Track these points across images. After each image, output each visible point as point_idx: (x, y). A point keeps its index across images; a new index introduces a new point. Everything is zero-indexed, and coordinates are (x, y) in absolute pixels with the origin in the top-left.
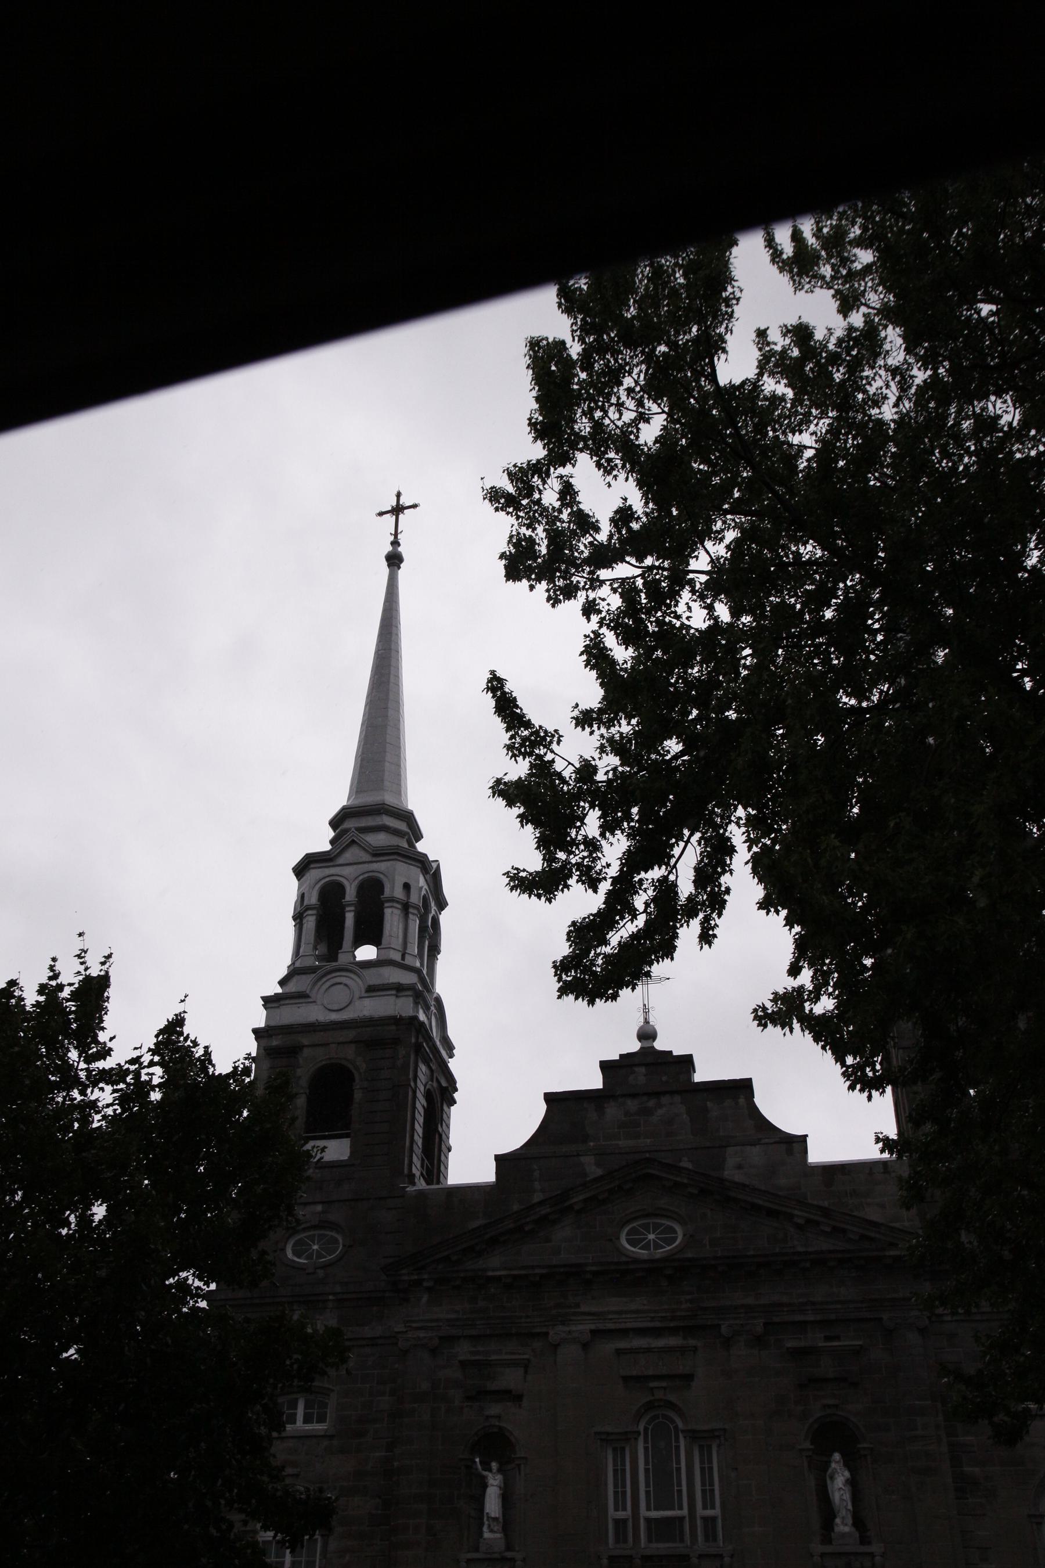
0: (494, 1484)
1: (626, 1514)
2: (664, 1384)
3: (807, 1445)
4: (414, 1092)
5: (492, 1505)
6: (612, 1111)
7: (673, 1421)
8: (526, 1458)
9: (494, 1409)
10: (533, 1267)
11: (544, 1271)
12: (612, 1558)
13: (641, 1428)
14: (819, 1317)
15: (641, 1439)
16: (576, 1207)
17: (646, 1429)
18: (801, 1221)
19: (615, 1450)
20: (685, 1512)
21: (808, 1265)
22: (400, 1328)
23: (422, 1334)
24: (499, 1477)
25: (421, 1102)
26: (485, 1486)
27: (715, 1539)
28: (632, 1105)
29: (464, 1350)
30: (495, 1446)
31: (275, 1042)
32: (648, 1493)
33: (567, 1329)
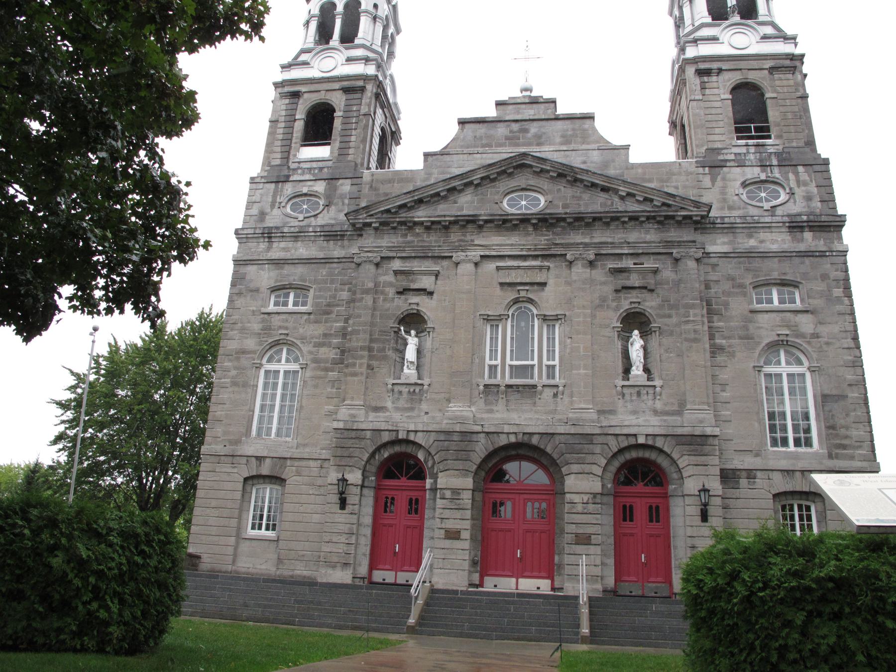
0: (412, 343)
2: (527, 288)
3: (619, 325)
4: (373, 121)
5: (411, 354)
6: (501, 131)
7: (531, 311)
9: (414, 299)
10: (445, 216)
14: (631, 251)
15: (509, 320)
16: (475, 182)
18: (624, 194)
19: (492, 326)
20: (535, 362)
21: (626, 219)
22: (356, 251)
23: (370, 255)
24: (416, 340)
25: (377, 131)
26: (406, 344)
27: (554, 378)
28: (515, 127)
30: (413, 321)
31: (286, 89)
32: (512, 351)
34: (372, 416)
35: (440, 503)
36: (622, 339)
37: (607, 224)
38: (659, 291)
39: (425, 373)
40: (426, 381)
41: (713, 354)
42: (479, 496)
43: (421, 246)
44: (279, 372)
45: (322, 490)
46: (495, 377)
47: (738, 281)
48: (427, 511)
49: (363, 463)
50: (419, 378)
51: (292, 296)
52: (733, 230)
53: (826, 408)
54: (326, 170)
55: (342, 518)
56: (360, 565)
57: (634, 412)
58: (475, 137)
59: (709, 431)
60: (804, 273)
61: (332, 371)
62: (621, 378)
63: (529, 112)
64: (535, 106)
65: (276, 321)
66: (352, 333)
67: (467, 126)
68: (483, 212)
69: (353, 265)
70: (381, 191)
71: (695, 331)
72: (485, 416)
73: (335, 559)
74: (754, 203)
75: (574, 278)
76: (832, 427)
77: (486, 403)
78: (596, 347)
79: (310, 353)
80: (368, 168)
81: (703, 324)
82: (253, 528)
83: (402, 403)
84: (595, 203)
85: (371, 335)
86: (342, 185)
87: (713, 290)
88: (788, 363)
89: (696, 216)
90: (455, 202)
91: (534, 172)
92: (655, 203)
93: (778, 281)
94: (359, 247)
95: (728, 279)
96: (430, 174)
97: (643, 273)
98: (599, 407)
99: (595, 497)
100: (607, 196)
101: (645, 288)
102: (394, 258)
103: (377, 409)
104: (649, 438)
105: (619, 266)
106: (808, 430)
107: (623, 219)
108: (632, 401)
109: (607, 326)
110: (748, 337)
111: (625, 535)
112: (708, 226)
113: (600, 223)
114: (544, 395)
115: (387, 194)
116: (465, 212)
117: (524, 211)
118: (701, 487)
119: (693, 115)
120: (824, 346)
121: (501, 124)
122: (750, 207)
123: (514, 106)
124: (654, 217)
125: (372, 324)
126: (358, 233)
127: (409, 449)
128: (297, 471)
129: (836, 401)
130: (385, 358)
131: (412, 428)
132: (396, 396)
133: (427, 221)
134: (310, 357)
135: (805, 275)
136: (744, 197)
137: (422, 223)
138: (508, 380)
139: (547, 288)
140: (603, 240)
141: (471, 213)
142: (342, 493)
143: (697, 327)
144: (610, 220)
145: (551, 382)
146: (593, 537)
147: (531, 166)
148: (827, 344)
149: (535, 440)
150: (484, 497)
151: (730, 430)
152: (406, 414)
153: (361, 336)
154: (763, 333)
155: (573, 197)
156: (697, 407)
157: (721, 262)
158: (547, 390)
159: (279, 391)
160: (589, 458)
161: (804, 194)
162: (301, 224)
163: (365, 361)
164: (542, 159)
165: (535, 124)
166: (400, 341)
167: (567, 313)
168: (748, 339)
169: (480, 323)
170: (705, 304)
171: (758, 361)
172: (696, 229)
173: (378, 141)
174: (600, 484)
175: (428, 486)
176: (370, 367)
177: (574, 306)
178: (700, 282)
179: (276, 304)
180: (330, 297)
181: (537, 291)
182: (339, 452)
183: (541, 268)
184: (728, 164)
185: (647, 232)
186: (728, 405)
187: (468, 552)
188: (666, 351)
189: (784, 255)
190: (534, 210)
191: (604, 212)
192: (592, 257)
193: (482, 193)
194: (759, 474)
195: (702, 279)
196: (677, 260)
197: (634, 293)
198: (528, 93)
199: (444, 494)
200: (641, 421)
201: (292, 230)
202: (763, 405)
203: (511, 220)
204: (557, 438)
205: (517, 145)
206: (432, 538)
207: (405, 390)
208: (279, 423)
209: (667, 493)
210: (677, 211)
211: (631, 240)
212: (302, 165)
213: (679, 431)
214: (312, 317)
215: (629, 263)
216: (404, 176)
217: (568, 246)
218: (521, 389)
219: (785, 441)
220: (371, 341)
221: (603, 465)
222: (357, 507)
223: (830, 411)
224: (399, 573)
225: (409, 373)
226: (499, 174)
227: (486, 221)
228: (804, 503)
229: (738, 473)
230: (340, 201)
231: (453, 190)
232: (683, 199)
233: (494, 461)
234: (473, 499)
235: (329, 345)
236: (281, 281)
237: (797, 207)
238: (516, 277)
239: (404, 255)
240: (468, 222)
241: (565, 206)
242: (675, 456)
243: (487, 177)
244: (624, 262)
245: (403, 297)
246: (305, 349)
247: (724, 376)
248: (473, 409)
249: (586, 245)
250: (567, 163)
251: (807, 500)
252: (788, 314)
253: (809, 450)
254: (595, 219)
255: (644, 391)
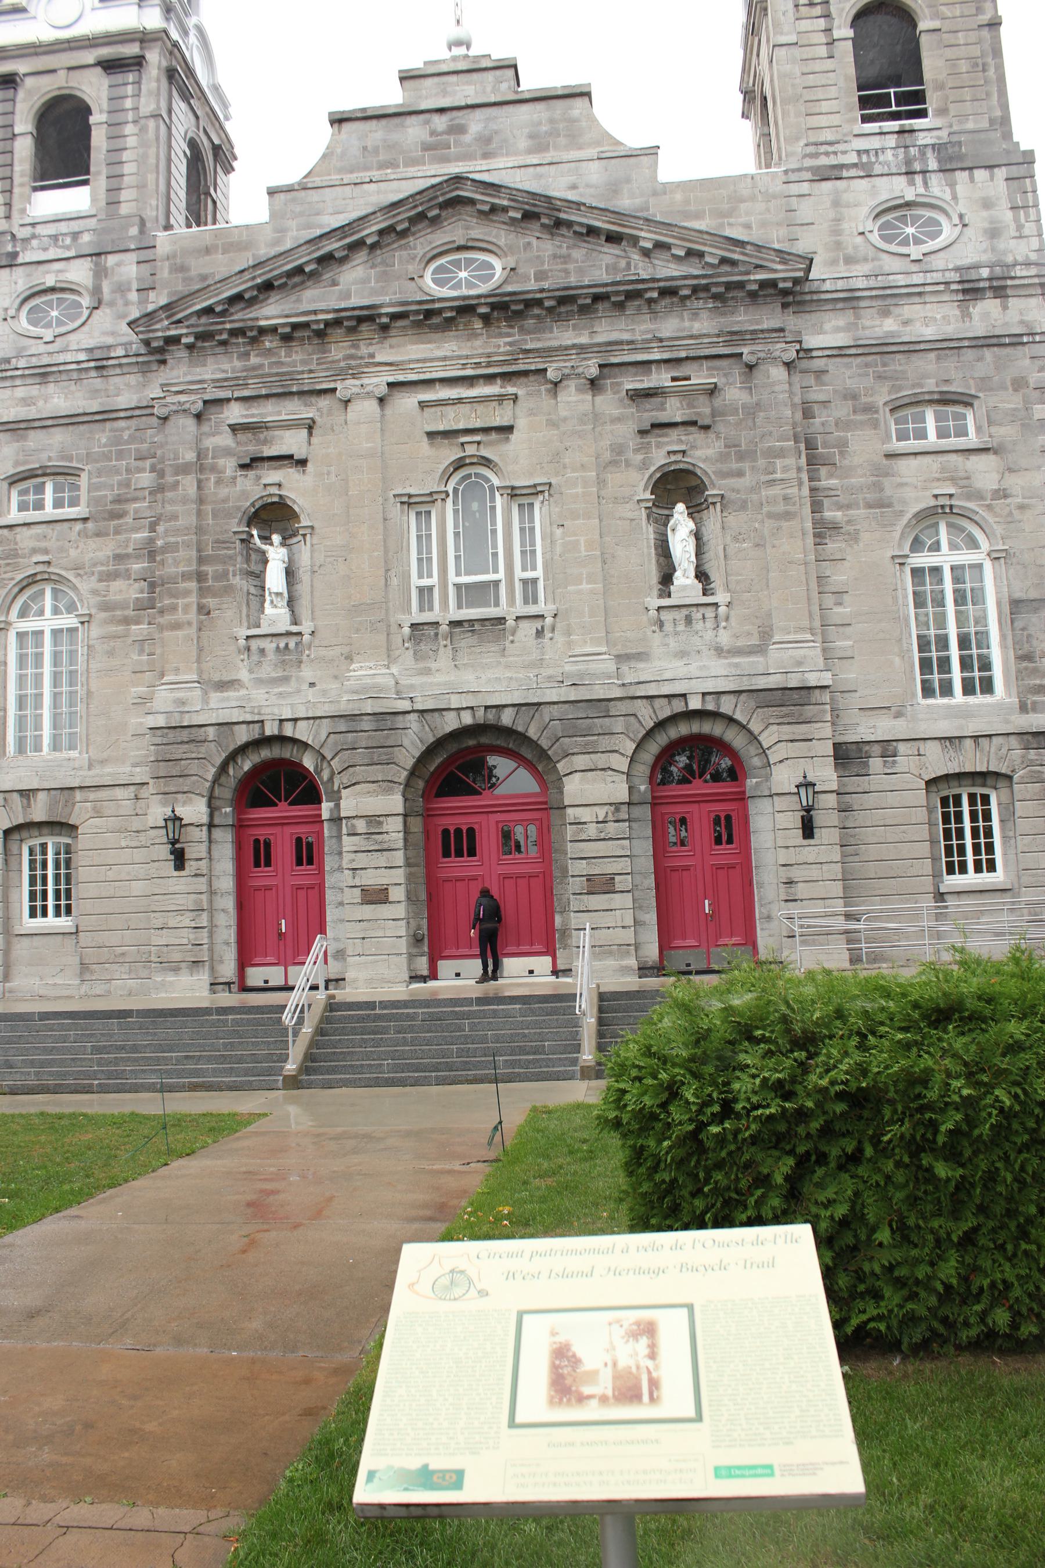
1: (434, 581)
2: (477, 438)
3: (648, 495)
4: (169, 128)
5: (275, 579)
6: (414, 132)
7: (488, 480)
8: (312, 527)
9: (272, 476)
10: (315, 312)
11: (330, 316)
12: (414, 626)
13: (450, 488)
14: (666, 356)
15: (450, 501)
16: (369, 241)
17: (456, 490)
18: (649, 245)
19: (418, 514)
20: (501, 575)
21: (655, 295)
22: (157, 393)
23: (182, 398)
24: (283, 551)
25: (180, 147)
26: (266, 562)
27: (535, 601)
28: (440, 122)
29: (235, 413)
30: (274, 516)
32: (457, 558)
33: (357, 382)
34: (215, 697)
35: (349, 843)
36: (656, 521)
37: (620, 306)
38: (720, 427)
39: (304, 613)
40: (306, 627)
41: (819, 537)
42: (417, 825)
43: (277, 374)
44: (42, 632)
45: (142, 837)
46: (431, 609)
47: (864, 400)
48: (327, 858)
49: (208, 785)
50: (295, 623)
51: (49, 488)
52: (855, 304)
53: (1019, 624)
54: (86, 238)
55: (180, 883)
56: (222, 962)
57: (682, 654)
58: (365, 148)
59: (813, 680)
60: (982, 379)
61: (138, 623)
62: (655, 592)
63: (466, 90)
64: (475, 76)
65: (25, 539)
66: (167, 548)
67: (347, 127)
68: (388, 298)
69: (154, 421)
70: (193, 273)
71: (786, 498)
72: (416, 680)
73: (176, 956)
74: (893, 248)
75: (563, 413)
76: (1028, 657)
77: (418, 656)
78: (607, 539)
79: (95, 592)
80: (168, 227)
81: (800, 484)
82: (33, 914)
83: (268, 670)
84: (598, 267)
85: (199, 551)
86: (119, 264)
87: (817, 420)
88: (953, 546)
89: (784, 280)
90: (335, 283)
91: (480, 212)
92: (708, 259)
93: (936, 397)
94: (162, 385)
95: (845, 398)
96: (282, 231)
97: (688, 395)
98: (619, 650)
99: (617, 810)
100: (617, 252)
101: (694, 423)
102: (228, 400)
103: (223, 685)
104: (708, 698)
105: (645, 385)
106: (986, 665)
107: (648, 295)
108: (676, 633)
109: (626, 500)
110: (881, 504)
111: (674, 869)
112: (808, 297)
113: (607, 305)
114: (520, 634)
115: (204, 278)
116: (355, 301)
117: (465, 292)
118: (801, 779)
119: (779, 77)
120: (1015, 512)
121: (414, 118)
122: (884, 256)
123: (436, 80)
124: (706, 288)
125: (200, 530)
126: (158, 357)
127: (287, 753)
128: (94, 809)
129: (1036, 610)
130: (229, 590)
131: (287, 714)
132: (255, 658)
133: (284, 325)
134: (94, 600)
135: (984, 383)
136: (875, 238)
137: (274, 329)
138: (456, 614)
139: (513, 437)
140: (615, 336)
141: (366, 302)
142: (174, 842)
143: (789, 491)
144: (625, 298)
145: (532, 610)
146: (617, 878)
147: (472, 202)
148: (1022, 507)
149: (507, 718)
150: (426, 825)
151: (850, 674)
152: (276, 690)
153: (182, 553)
154: (909, 493)
155: (555, 256)
156: (791, 637)
157: (832, 365)
158: (524, 624)
159: (47, 669)
160: (605, 743)
161: (986, 225)
162: (50, 348)
163: (193, 599)
164: (492, 185)
165: (479, 113)
166: (254, 556)
167: (553, 481)
168: (882, 506)
169: (395, 510)
170: (802, 446)
171: (900, 546)
172: (785, 306)
173: (183, 168)
174: (625, 786)
175: (325, 815)
176: (204, 610)
177: (565, 467)
178: (793, 405)
179: (23, 507)
180: (120, 484)
181: (499, 441)
182: (163, 769)
183: (501, 399)
184: (845, 174)
185: (695, 316)
186: (847, 629)
187: (403, 923)
188: (736, 539)
189: (947, 347)
190: (483, 289)
191: (613, 284)
192: (594, 371)
193: (384, 263)
194: (902, 748)
195: (797, 400)
196: (750, 367)
197: (674, 434)
198: (461, 51)
199: (353, 826)
200: (692, 669)
201: (34, 361)
202: (908, 625)
203: (439, 312)
204: (546, 712)
205: (446, 160)
206: (341, 904)
207: (269, 645)
208: (55, 726)
209: (744, 792)
210: (748, 273)
211: (665, 334)
212: (40, 230)
213: (761, 683)
214: (90, 525)
215: (661, 378)
216: (238, 241)
217: (547, 353)
218: (477, 627)
219: (947, 689)
220: (201, 560)
221: (630, 753)
222: (203, 864)
223: (1023, 629)
224: (290, 968)
225: (275, 615)
226: (413, 220)
227: (395, 317)
228: (979, 791)
229: (867, 748)
230: (118, 295)
231: (327, 259)
232: (759, 247)
233: (438, 761)
234: (406, 831)
235: (127, 575)
236: (25, 463)
237: (973, 252)
238: (456, 419)
239: (246, 393)
240: (360, 320)
241: (540, 276)
242: (755, 727)
243: (390, 230)
244: (654, 376)
245: (251, 473)
246: (85, 586)
247: (839, 577)
248: (394, 670)
249: (582, 349)
250: (538, 191)
251: (984, 785)
252: (953, 457)
253: (987, 699)
254: (597, 298)
255: (697, 615)
